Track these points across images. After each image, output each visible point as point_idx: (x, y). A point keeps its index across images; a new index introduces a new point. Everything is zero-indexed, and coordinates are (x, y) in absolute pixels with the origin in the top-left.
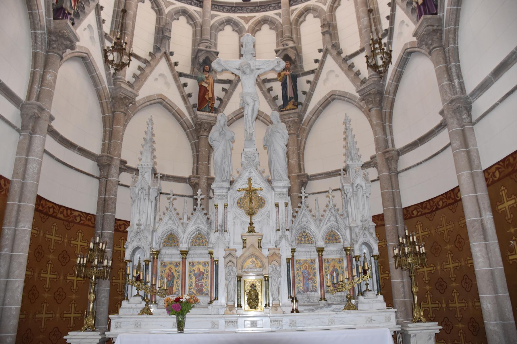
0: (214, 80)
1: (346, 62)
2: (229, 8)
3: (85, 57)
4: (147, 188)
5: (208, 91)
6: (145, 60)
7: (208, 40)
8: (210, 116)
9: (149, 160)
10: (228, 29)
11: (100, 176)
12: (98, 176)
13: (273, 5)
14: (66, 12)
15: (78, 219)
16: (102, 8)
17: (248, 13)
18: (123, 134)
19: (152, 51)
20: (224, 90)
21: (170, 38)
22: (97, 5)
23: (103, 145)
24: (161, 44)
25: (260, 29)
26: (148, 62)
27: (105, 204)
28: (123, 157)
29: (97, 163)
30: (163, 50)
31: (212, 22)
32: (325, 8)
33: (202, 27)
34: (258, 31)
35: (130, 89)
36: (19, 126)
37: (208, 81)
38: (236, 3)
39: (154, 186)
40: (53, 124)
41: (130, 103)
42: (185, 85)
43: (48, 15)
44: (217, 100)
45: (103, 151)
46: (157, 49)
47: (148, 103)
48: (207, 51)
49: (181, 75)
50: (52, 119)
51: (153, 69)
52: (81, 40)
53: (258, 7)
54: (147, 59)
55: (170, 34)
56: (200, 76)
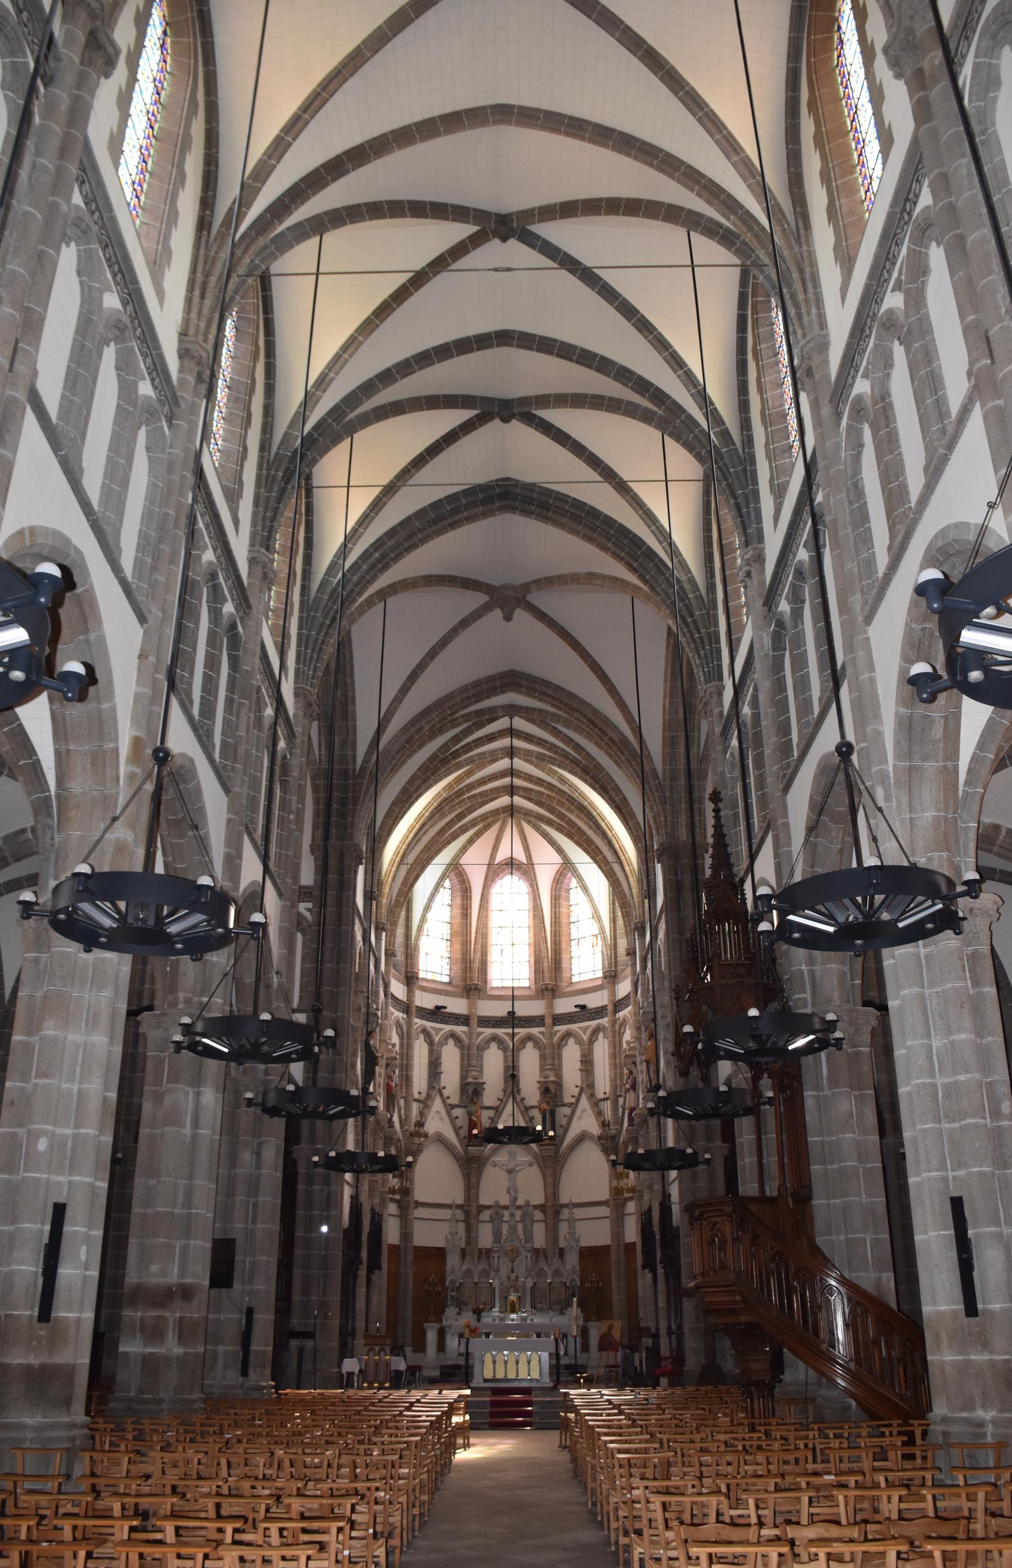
1: (596, 1103)
10: (494, 1046)
32: (585, 1038)
46: (431, 1087)
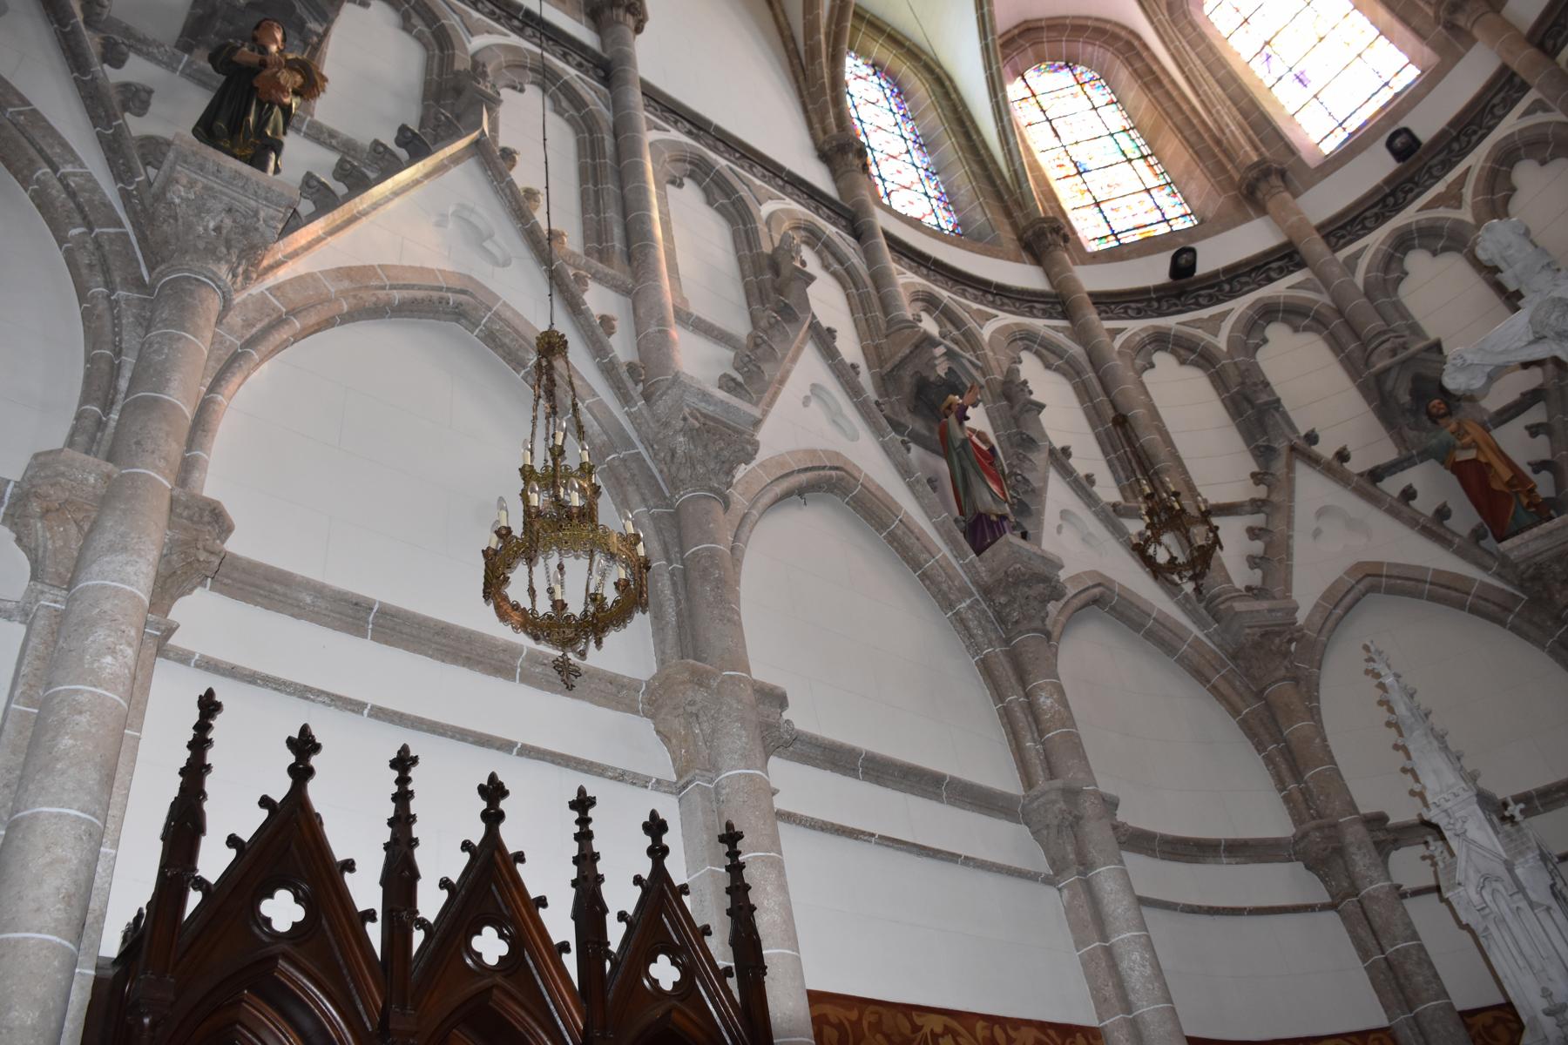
0: (1483, 425)
2: (1376, 210)
3: (1102, 595)
4: (1501, 870)
5: (1489, 465)
6: (1253, 501)
7: (1385, 332)
8: (1550, 533)
9: (1450, 777)
10: (1418, 262)
11: (1332, 896)
12: (1327, 899)
13: (1496, 100)
14: (994, 518)
16: (1066, 451)
17: (1438, 179)
18: (1324, 739)
19: (1256, 469)
20: (1534, 430)
21: (1278, 400)
22: (1052, 452)
23: (1287, 800)
24: (1265, 432)
25: (1513, 190)
26: (1264, 502)
27: (1396, 978)
28: (1366, 807)
29: (1300, 865)
30: (1281, 445)
31: (1359, 279)
33: (1340, 312)
34: (1507, 199)
35: (1264, 605)
36: (1044, 867)
37: (1467, 440)
38: (1387, 181)
39: (1521, 853)
40: (1121, 816)
41: (1290, 641)
42: (1408, 494)
43: (960, 555)
44: (1536, 471)
45: (1298, 820)
46: (1264, 454)
47: (1339, 611)
48: (1403, 362)
49: (1375, 475)
50: (1111, 804)
51: (1290, 510)
52: (1065, 562)
53: (1457, 139)
54: (1257, 496)
55: (1273, 393)
56: (1434, 441)
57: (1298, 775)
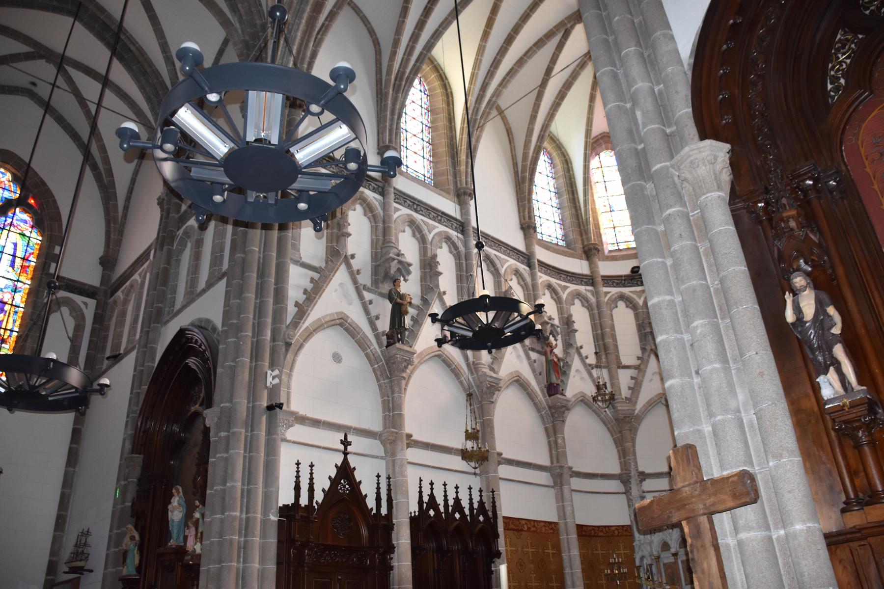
15: (616, 532)
23: (621, 463)
36: (552, 484)
43: (545, 397)
46: (643, 349)
51: (645, 371)
57: (624, 458)
